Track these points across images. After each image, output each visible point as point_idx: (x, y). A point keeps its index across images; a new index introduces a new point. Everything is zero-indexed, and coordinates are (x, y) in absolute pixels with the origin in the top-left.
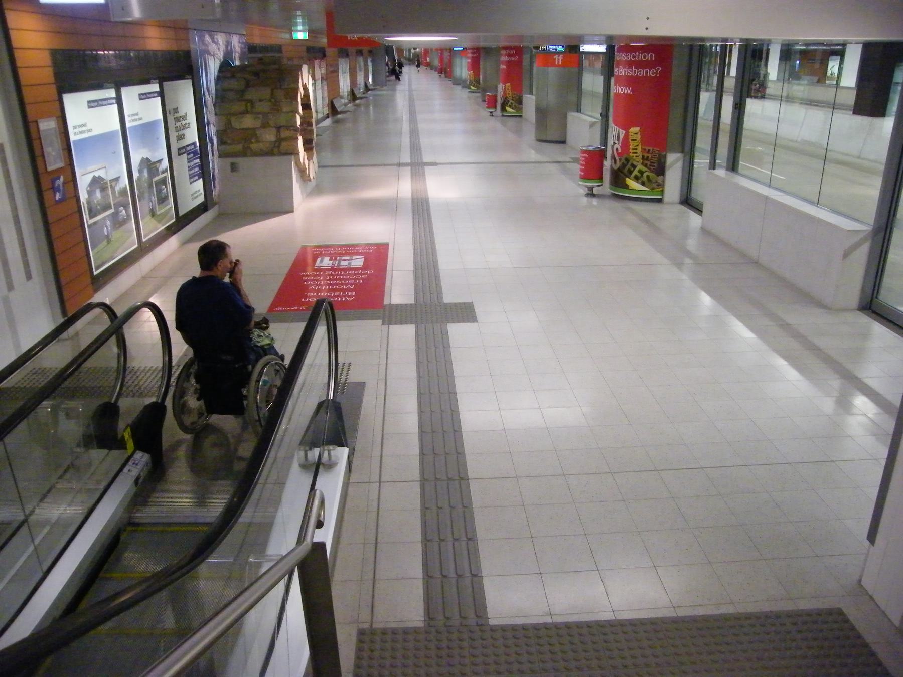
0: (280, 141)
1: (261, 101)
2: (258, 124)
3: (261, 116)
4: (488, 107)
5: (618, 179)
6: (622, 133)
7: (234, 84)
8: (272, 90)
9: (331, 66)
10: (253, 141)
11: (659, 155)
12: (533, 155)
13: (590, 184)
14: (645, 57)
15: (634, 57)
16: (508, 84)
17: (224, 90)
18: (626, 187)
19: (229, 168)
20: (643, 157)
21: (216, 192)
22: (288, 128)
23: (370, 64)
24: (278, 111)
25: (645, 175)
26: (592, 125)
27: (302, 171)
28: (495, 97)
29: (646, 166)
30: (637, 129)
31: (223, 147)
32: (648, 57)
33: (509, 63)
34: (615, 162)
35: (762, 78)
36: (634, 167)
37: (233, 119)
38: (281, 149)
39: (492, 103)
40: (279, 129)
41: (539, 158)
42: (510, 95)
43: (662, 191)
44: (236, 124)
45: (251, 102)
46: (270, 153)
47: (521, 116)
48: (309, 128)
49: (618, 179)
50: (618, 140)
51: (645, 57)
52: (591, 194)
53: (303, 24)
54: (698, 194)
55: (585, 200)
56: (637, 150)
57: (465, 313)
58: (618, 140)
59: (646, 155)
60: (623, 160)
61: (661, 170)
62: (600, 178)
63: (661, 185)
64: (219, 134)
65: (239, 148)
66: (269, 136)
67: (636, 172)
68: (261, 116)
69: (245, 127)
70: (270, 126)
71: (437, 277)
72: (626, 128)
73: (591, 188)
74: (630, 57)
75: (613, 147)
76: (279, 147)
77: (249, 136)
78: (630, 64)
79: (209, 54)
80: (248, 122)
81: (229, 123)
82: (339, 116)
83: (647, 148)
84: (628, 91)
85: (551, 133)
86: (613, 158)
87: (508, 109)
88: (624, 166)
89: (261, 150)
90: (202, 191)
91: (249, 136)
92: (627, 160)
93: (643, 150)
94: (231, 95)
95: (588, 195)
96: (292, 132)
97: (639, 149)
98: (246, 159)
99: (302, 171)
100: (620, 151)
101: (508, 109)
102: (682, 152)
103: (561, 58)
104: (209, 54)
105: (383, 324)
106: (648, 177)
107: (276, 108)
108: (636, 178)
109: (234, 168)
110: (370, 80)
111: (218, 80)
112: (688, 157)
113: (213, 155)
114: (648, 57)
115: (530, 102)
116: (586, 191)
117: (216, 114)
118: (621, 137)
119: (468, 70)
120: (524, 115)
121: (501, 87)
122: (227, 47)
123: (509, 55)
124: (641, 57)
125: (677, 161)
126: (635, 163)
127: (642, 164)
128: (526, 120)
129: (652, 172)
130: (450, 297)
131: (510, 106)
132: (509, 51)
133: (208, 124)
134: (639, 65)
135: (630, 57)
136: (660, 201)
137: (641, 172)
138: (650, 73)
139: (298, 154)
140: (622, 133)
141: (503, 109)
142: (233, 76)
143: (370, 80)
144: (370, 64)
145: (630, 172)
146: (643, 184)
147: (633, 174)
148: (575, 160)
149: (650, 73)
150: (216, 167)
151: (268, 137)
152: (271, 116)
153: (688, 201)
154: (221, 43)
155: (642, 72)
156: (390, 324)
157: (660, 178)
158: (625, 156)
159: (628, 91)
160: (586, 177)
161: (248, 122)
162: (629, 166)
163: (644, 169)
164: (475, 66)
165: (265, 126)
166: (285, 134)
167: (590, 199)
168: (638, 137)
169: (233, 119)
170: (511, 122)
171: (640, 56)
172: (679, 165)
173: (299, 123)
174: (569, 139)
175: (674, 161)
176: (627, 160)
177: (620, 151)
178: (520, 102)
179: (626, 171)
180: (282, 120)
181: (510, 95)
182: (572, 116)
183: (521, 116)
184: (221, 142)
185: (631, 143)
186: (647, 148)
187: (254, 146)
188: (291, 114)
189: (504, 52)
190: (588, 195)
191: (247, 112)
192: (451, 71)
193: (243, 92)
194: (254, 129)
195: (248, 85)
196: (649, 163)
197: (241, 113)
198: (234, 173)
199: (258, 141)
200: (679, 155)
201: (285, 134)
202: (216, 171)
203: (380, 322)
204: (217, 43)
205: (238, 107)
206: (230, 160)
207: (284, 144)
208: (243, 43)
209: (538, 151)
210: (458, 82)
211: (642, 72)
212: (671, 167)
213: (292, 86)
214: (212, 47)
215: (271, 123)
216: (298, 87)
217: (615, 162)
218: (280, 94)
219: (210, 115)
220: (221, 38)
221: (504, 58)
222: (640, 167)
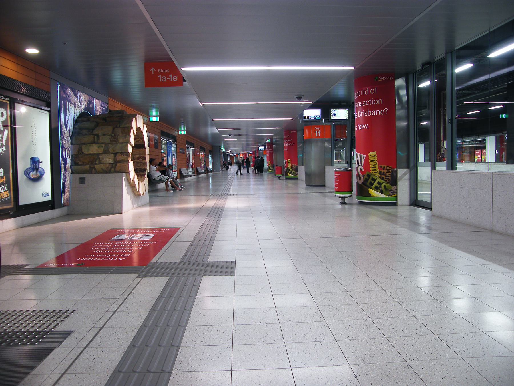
0: (116, 162)
1: (104, 135)
2: (101, 150)
3: (103, 145)
4: (277, 174)
5: (363, 191)
6: (364, 156)
7: (87, 124)
8: (114, 129)
9: (180, 149)
10: (97, 163)
11: (392, 171)
12: (304, 191)
13: (342, 195)
14: (376, 102)
15: (368, 103)
17: (81, 129)
18: (369, 195)
19: (78, 181)
20: (380, 172)
21: (65, 197)
22: (121, 153)
23: (210, 158)
24: (115, 141)
25: (382, 185)
27: (132, 186)
29: (383, 179)
30: (374, 153)
31: (76, 167)
32: (378, 102)
33: (289, 147)
34: (360, 179)
35: (442, 152)
36: (374, 180)
37: (83, 147)
38: (118, 168)
39: (280, 171)
40: (115, 154)
41: (307, 192)
43: (396, 197)
44: (85, 151)
45: (97, 135)
46: (108, 171)
48: (144, 161)
49: (363, 191)
50: (361, 162)
51: (376, 102)
52: (344, 203)
53: (157, 111)
54: (424, 195)
55: (340, 206)
56: (375, 167)
57: (228, 269)
58: (361, 162)
59: (382, 171)
60: (366, 176)
61: (394, 181)
62: (350, 190)
63: (395, 192)
64: (73, 157)
65: (87, 167)
66: (108, 159)
67: (376, 184)
68: (103, 145)
69: (91, 152)
70: (109, 152)
71: (210, 245)
72: (366, 153)
73: (343, 199)
74: (365, 103)
75: (357, 168)
76: (115, 168)
77: (94, 159)
78: (365, 108)
79: (70, 101)
80: (94, 149)
81: (80, 149)
82: (186, 179)
83: (383, 166)
84: (366, 127)
85: (316, 181)
86: (358, 175)
88: (366, 180)
89: (103, 170)
90: (50, 194)
91: (94, 159)
92: (369, 176)
93: (380, 168)
94: (85, 132)
95: (341, 203)
96: (125, 156)
97: (377, 166)
98: (90, 175)
99: (132, 186)
100: (363, 170)
102: (408, 167)
103: (319, 132)
104: (70, 101)
105: (138, 277)
106: (385, 186)
107: (114, 140)
108: (377, 189)
109: (82, 181)
110: (210, 167)
111: (76, 122)
112: (413, 171)
113: (65, 170)
114: (378, 102)
115: (302, 170)
116: (340, 200)
117: (72, 144)
118: (363, 160)
120: (299, 178)
121: (285, 161)
122: (89, 104)
123: (289, 142)
124: (373, 102)
125: (404, 175)
126: (374, 177)
127: (380, 177)
129: (387, 183)
130: (216, 256)
131: (290, 173)
132: (289, 140)
133: (63, 147)
134: (372, 108)
135: (365, 103)
136: (395, 204)
137: (379, 183)
138: (380, 113)
139: (129, 172)
140: (364, 156)
142: (89, 120)
143: (210, 167)
144: (210, 158)
145: (372, 184)
146: (382, 192)
147: (374, 186)
148: (331, 192)
149: (380, 113)
150: (67, 179)
151: (107, 159)
152: (110, 145)
153: (415, 203)
154: (83, 100)
155: (375, 113)
156: (145, 276)
157: (394, 188)
158: (367, 173)
159: (366, 127)
160: (339, 190)
161: (94, 149)
162: (370, 180)
163: (382, 181)
165: (106, 152)
166: (120, 157)
167: (343, 205)
168: (376, 158)
169: (83, 147)
170: (290, 184)
171: (372, 102)
172: (407, 177)
173: (130, 150)
175: (403, 174)
176: (369, 176)
177: (363, 170)
178: (296, 170)
179: (368, 183)
180: (118, 147)
183: (297, 179)
184: (74, 163)
185: (370, 163)
186: (383, 166)
187: (97, 166)
188: (125, 144)
189: (286, 141)
190: (341, 203)
191: (94, 142)
193: (93, 130)
194: (98, 154)
195: (97, 125)
196: (384, 176)
197: (89, 143)
198: (82, 185)
199: (100, 163)
200: (406, 170)
201: (120, 157)
202: (68, 182)
203: (137, 275)
204: (79, 98)
205: (87, 139)
206: (78, 176)
207: (118, 164)
208: (104, 107)
209: (306, 189)
211: (375, 113)
212: (401, 179)
213: (127, 125)
214: (73, 98)
215: (110, 150)
216: (131, 127)
217: (360, 179)
218: (119, 131)
219: (65, 140)
220: (84, 98)
221: (286, 145)
222: (378, 180)
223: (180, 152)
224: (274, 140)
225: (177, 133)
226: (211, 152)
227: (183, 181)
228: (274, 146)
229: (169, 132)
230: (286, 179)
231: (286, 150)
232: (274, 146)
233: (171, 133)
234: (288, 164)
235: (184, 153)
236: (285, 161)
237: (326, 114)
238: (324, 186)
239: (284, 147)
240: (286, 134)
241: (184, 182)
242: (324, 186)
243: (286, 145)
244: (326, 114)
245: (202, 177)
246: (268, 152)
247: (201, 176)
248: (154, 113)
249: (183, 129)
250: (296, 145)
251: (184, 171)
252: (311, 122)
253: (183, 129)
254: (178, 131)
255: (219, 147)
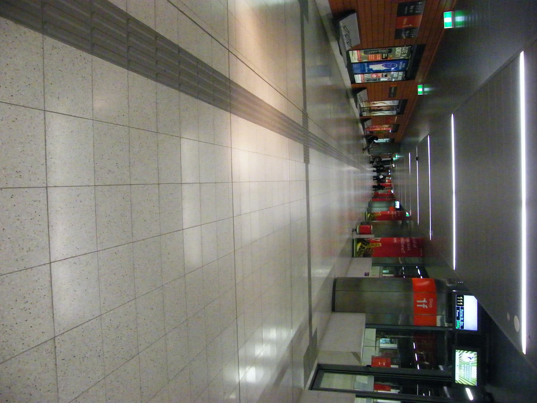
4: (360, 228)
9: (396, 88)
16: (380, 244)
26: (357, 355)
28: (371, 234)
33: (399, 245)
39: (364, 230)
41: (315, 293)
42: (371, 246)
47: (353, 256)
82: (352, 101)
85: (344, 296)
87: (359, 245)
101: (359, 245)
103: (424, 306)
119: (382, 212)
120: (355, 259)
121: (379, 239)
123: (406, 245)
128: (350, 262)
131: (361, 246)
141: (359, 240)
164: (384, 217)
174: (338, 317)
178: (366, 255)
181: (371, 246)
182: (361, 318)
183: (353, 256)
189: (408, 241)
192: (377, 200)
210: (370, 206)
223: (391, 88)
224: (408, 222)
225: (420, 81)
226: (392, 141)
227: (350, 95)
228: (400, 222)
229: (420, 68)
230: (353, 240)
231: (395, 240)
232: (400, 222)
233: (418, 73)
234: (374, 244)
235: (390, 96)
236: (379, 239)
237: (467, 340)
238: (334, 309)
239: (399, 236)
240: (418, 240)
241: (348, 98)
242: (334, 309)
243: (402, 240)
244: (467, 340)
245: (358, 128)
246: (392, 213)
247: (360, 126)
248: (460, 19)
249: (426, 89)
250: (401, 255)
251: (363, 94)
252: (453, 310)
253: (426, 89)
254: (424, 84)
255: (399, 152)
